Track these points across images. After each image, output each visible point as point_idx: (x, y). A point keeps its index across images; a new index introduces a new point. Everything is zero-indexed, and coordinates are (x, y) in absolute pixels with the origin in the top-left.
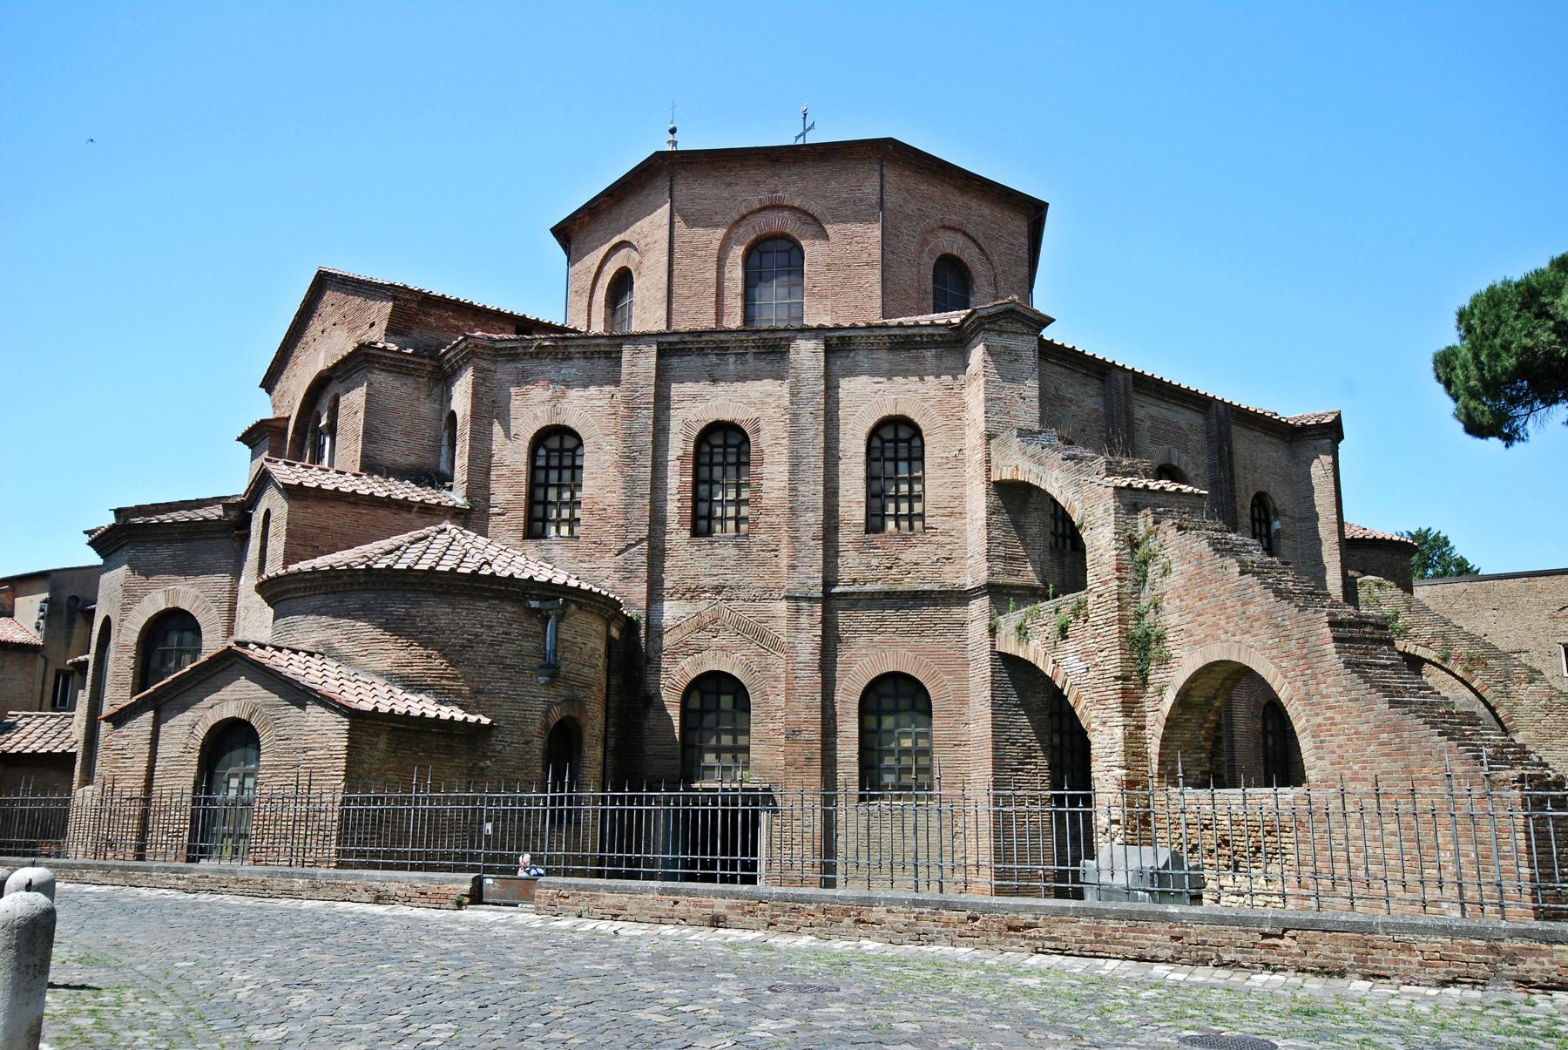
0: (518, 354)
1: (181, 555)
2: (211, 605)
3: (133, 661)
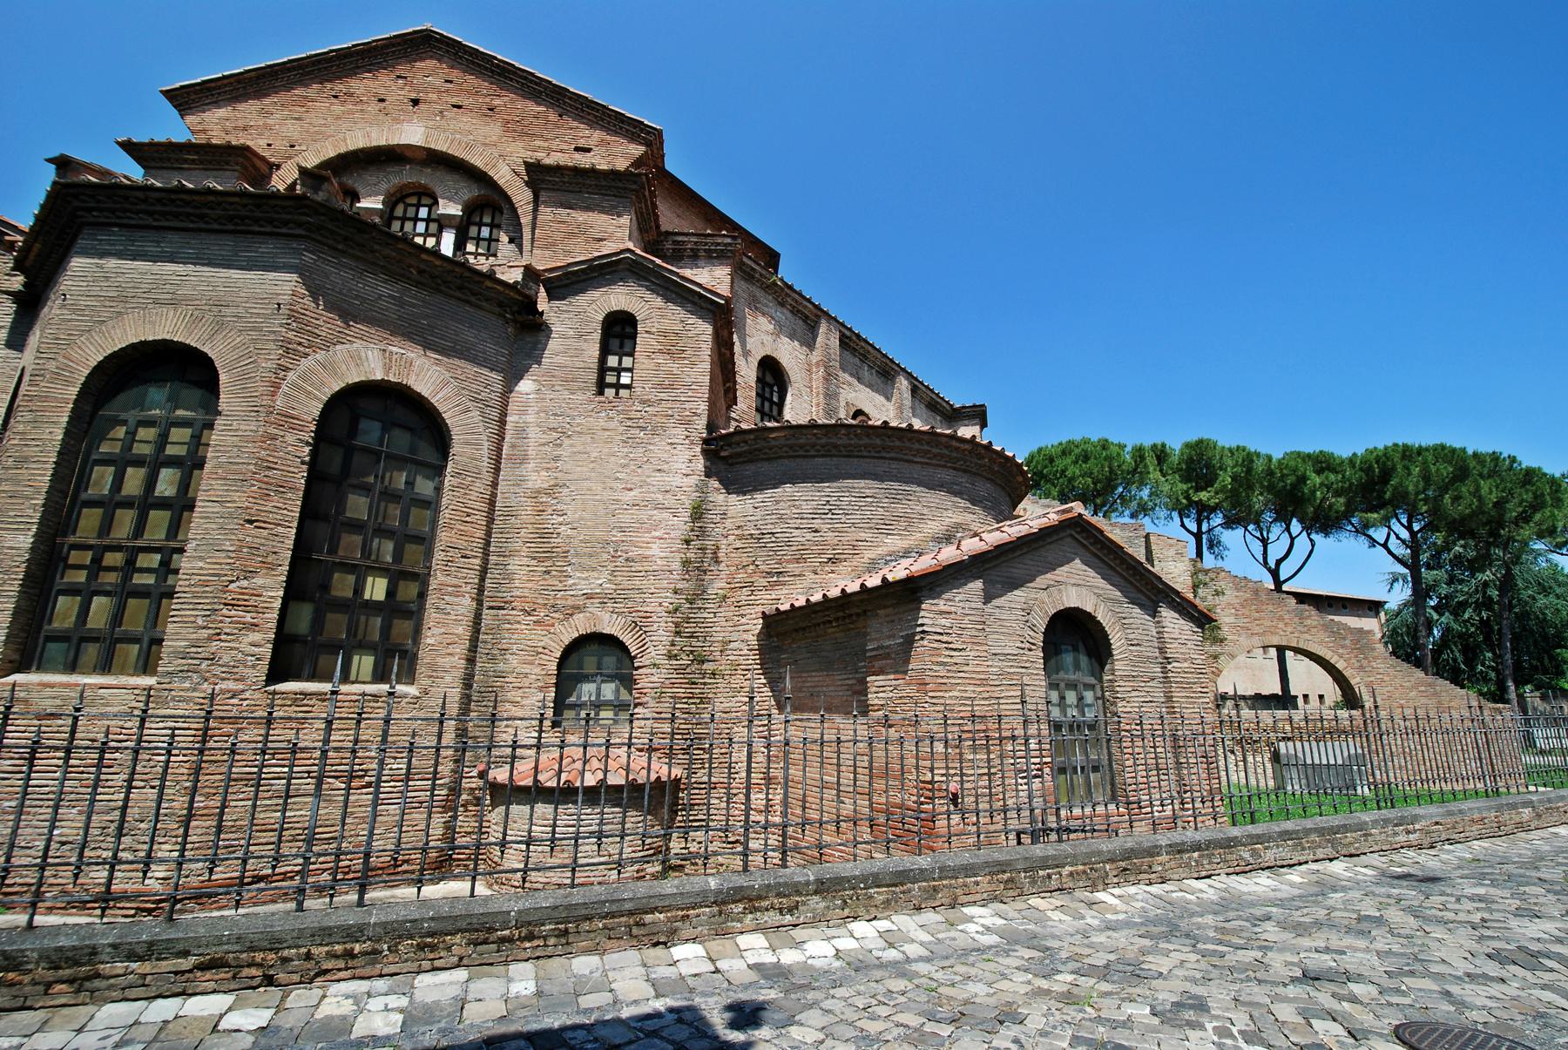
0: (753, 277)
1: (414, 306)
2: (470, 404)
3: (307, 449)
